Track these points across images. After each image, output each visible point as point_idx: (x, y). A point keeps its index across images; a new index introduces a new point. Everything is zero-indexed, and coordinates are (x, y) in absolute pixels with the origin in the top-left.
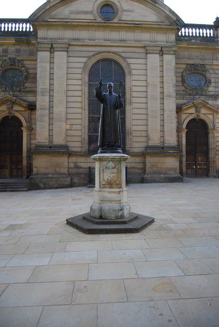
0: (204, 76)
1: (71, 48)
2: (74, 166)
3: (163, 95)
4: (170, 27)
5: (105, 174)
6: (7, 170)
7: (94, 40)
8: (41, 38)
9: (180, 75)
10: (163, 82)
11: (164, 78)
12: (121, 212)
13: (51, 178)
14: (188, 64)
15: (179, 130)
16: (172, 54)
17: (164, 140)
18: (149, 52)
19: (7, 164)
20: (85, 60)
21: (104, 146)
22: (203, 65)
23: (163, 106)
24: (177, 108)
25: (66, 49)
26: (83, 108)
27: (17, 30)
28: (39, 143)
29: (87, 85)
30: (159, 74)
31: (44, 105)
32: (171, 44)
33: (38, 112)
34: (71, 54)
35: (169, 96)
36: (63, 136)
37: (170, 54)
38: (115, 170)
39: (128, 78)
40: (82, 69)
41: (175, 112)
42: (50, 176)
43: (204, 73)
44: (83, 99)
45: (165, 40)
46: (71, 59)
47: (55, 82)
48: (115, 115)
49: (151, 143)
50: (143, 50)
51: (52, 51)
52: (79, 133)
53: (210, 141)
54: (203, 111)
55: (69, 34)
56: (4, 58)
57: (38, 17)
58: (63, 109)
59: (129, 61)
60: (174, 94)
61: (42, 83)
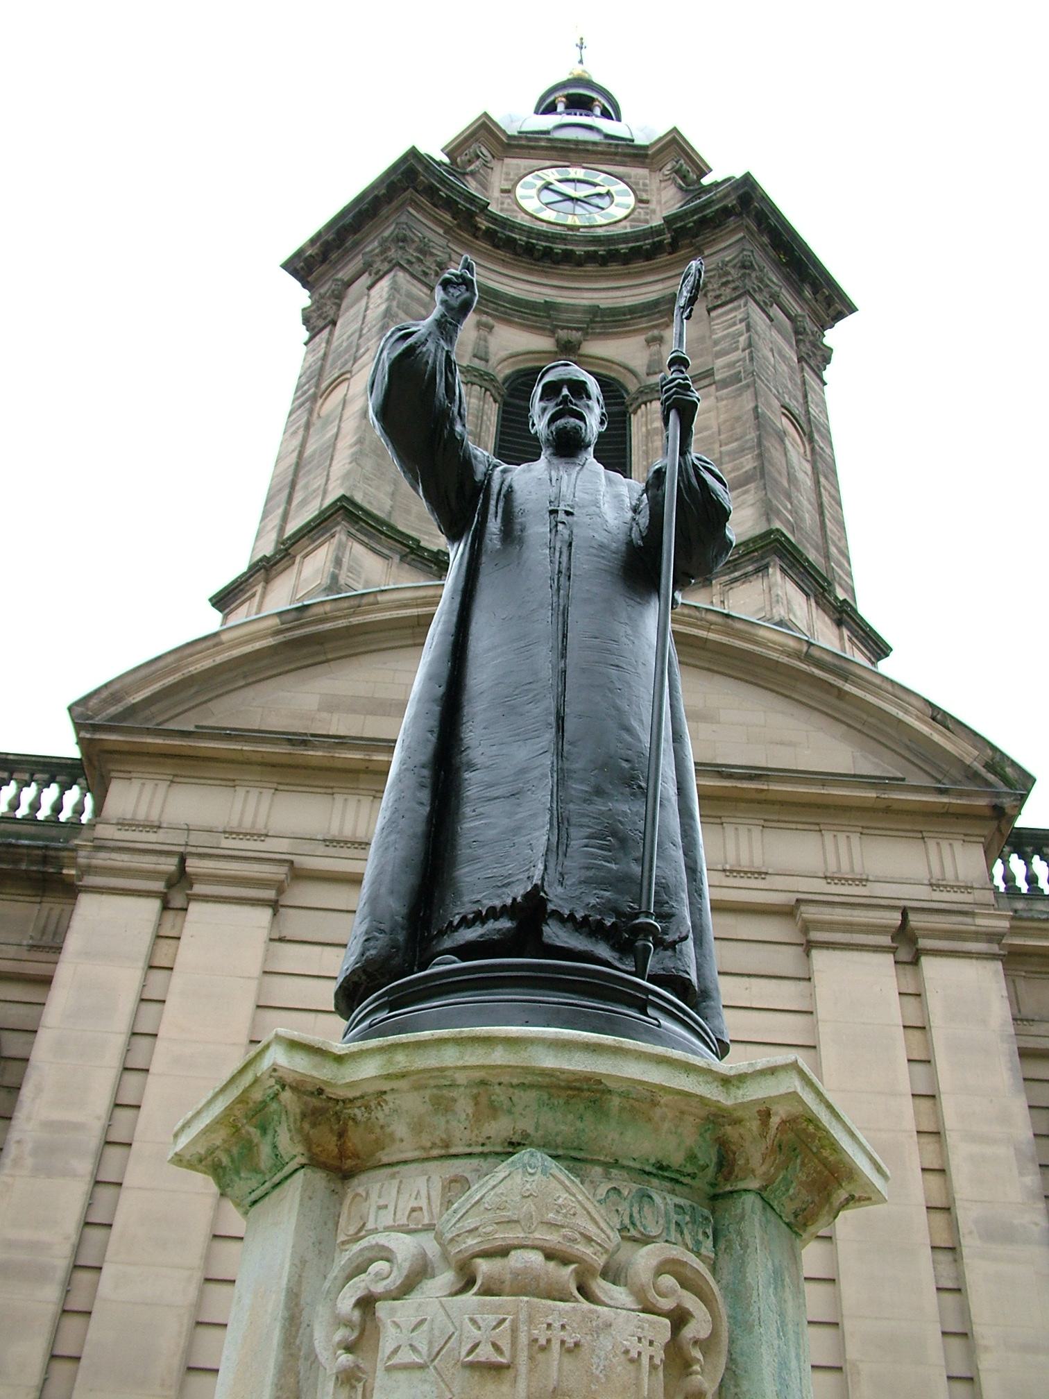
3: (954, 1227)
8: (122, 824)
10: (937, 1133)
18: (816, 936)
23: (964, 1312)
25: (270, 894)
30: (904, 1078)
31: (34, 1246)
34: (296, 923)
35: (1000, 1233)
37: (967, 955)
45: (923, 875)
51: (177, 901)
57: (132, 710)
58: (177, 1289)
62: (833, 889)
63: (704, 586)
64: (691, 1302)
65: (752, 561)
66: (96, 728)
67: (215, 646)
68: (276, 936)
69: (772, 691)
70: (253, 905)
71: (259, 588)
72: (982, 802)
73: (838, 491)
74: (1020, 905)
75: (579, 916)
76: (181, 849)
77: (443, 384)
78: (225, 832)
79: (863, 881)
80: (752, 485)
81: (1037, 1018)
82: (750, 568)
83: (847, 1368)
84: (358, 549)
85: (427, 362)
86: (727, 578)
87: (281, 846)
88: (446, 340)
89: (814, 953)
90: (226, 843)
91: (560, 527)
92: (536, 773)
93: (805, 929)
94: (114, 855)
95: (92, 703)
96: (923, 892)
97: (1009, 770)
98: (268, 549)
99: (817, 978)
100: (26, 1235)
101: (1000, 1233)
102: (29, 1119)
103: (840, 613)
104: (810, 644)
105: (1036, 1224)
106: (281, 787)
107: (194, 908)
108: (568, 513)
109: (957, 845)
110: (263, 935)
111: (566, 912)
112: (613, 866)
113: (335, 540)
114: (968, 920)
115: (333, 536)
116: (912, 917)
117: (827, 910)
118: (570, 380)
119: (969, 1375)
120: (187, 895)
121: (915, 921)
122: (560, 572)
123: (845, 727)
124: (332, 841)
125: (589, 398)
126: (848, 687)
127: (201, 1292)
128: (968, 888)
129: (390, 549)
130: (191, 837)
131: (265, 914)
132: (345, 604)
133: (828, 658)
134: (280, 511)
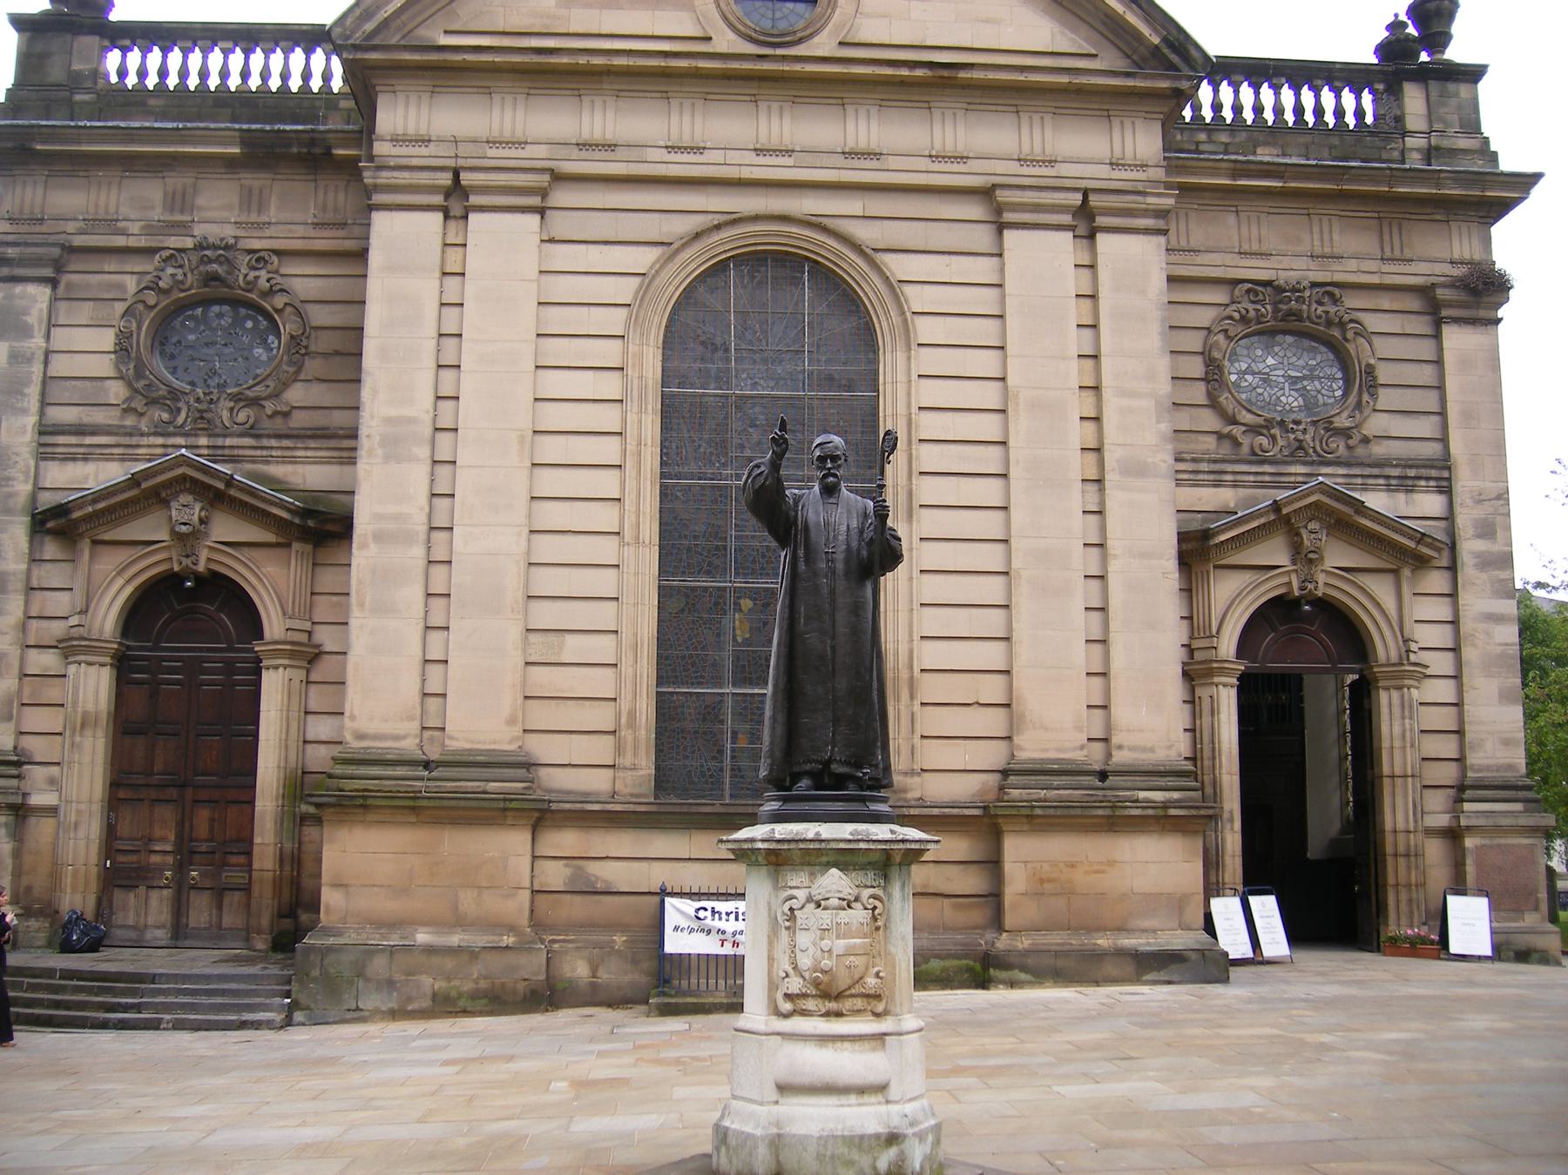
1: (563, 197)
2: (572, 879)
4: (1130, 83)
5: (803, 939)
6: (155, 895)
7: (699, 150)
8: (396, 140)
9: (1194, 342)
10: (1096, 388)
11: (1105, 362)
12: (893, 1152)
13: (430, 950)
14: (1236, 282)
15: (1195, 673)
16: (1147, 231)
17: (1108, 726)
18: (1009, 217)
19: (155, 859)
20: (644, 259)
21: (795, 778)
22: (1330, 291)
23: (1103, 529)
24: (1183, 537)
25: (535, 201)
26: (628, 534)
27: (254, 82)
28: (361, 736)
29: (654, 404)
31: (396, 517)
32: (1140, 175)
33: (364, 555)
34: (561, 224)
35: (1136, 470)
36: (508, 701)
38: (858, 915)
39: (893, 366)
40: (624, 311)
41: (1171, 564)
42: (422, 937)
43: (1336, 333)
44: (631, 484)
46: (563, 257)
47: (469, 385)
49: (1032, 747)
50: (974, 210)
51: (456, 210)
52: (601, 683)
54: (1338, 555)
55: (546, 125)
56: (174, 242)
57: (386, 23)
58: (511, 542)
59: (899, 267)
60: (1163, 459)
61: (393, 387)
62: (1026, 171)
64: (877, 903)
66: (356, 48)
74: (1202, 137)
76: (451, 163)
79: (1052, 162)
83: (1012, 573)
87: (541, 151)
89: (1006, 232)
90: (492, 152)
93: (999, 209)
94: (395, 174)
95: (349, 21)
96: (1104, 171)
99: (1006, 254)
100: (390, 509)
102: (372, 417)
107: (472, 217)
114: (1140, 199)
116: (1091, 197)
117: (1019, 193)
121: (1094, 200)
131: (535, 219)
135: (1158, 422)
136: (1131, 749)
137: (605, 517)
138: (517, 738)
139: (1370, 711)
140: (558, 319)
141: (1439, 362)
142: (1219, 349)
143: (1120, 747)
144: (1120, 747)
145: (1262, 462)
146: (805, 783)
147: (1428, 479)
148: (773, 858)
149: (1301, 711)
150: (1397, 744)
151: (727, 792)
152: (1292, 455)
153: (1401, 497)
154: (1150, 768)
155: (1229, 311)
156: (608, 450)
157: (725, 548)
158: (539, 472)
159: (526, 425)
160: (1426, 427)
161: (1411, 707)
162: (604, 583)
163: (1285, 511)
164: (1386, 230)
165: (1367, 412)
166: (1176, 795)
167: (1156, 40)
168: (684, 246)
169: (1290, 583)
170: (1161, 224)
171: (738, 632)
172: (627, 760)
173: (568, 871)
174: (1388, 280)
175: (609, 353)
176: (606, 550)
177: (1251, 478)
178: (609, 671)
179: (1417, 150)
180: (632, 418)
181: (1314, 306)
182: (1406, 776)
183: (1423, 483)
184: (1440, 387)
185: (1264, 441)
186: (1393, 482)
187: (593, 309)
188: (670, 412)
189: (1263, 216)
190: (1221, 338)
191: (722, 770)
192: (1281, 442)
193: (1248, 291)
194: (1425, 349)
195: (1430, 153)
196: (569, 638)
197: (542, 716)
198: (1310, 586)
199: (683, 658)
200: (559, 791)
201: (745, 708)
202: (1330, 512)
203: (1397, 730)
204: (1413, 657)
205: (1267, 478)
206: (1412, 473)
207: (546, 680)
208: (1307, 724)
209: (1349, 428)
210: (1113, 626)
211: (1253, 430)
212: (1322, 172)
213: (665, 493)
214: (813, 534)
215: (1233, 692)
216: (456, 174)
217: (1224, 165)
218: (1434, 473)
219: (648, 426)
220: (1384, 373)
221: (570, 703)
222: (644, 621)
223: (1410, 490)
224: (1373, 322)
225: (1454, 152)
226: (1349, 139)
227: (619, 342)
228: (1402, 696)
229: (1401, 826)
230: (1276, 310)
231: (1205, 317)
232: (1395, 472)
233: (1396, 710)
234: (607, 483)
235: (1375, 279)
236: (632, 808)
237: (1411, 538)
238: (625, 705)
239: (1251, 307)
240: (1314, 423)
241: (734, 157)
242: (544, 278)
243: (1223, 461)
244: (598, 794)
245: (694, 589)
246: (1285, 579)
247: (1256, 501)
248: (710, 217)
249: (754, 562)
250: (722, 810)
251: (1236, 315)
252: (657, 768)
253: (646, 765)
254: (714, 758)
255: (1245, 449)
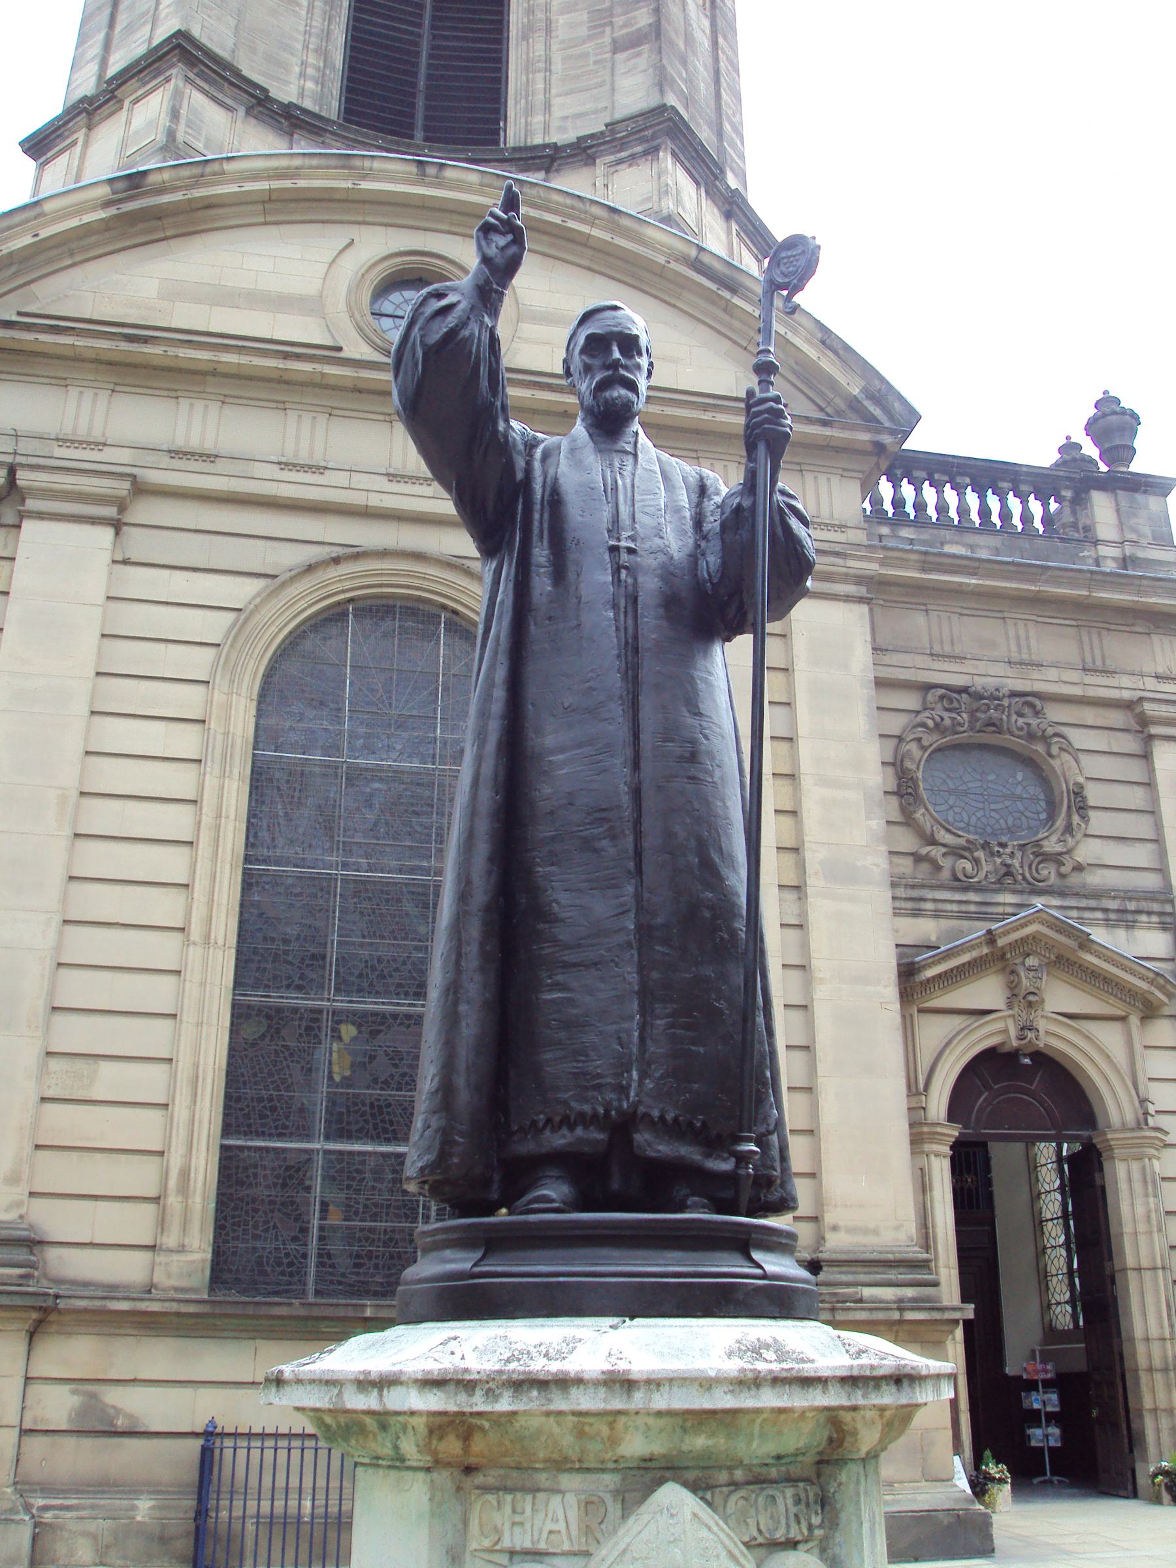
0: (1031, 763)
1: (146, 511)
3: (801, 867)
7: (320, 469)
11: (805, 748)
14: (928, 687)
15: (918, 1137)
16: (848, 599)
20: (242, 591)
22: (1031, 701)
23: (805, 946)
25: (111, 512)
26: (196, 933)
29: (241, 769)
34: (139, 543)
35: (843, 873)
37: (834, 597)
41: (889, 991)
43: (1040, 748)
44: (203, 868)
46: (139, 582)
48: (689, 698)
52: (144, 1129)
53: (1125, 1209)
54: (1061, 997)
55: (134, 425)
63: (586, 165)
65: (646, 140)
67: (35, 218)
68: (120, 559)
69: (656, 297)
70: (93, 523)
71: (80, 135)
72: (865, 437)
73: (737, 55)
74: (885, 530)
75: (670, 1116)
76: (9, 459)
77: (486, 374)
78: (57, 440)
80: (645, 48)
81: (890, 648)
82: (639, 149)
84: (198, 98)
85: (471, 352)
86: (612, 158)
88: (490, 316)
91: (624, 573)
92: (621, 938)
97: (897, 405)
98: (87, 86)
101: (843, 873)
103: (730, 203)
104: (701, 249)
105: (877, 866)
106: (118, 388)
107: (28, 526)
108: (631, 551)
109: (835, 480)
110: (106, 557)
111: (656, 1113)
112: (702, 1050)
113: (171, 86)
114: (839, 561)
115: (168, 80)
118: (620, 333)
119: (803, 1003)
120: (19, 511)
122: (627, 643)
123: (728, 343)
124: (177, 452)
125: (640, 354)
126: (736, 301)
127: (61, 934)
128: (842, 527)
129: (235, 99)
130: (19, 444)
131: (107, 533)
132: (185, 172)
133: (718, 266)
134: (101, 36)
135: (868, 818)
136: (851, 1231)
137: (164, 907)
138: (19, 1204)
139: (1103, 1188)
140: (126, 656)
141: (1150, 785)
142: (912, 759)
143: (835, 1228)
144: (835, 1228)
145: (966, 889)
146: (554, 1190)
147: (1149, 913)
148: (451, 1446)
149: (990, 1196)
150: (1142, 1228)
151: (311, 1286)
152: (999, 882)
153: (1121, 933)
154: (875, 1256)
155: (919, 719)
156: (176, 822)
157: (324, 957)
158: (82, 844)
159: (68, 775)
160: (1141, 855)
161: (1154, 1182)
162: (157, 993)
163: (1000, 943)
164: (1085, 638)
165: (1079, 836)
166: (909, 1292)
167: (856, 391)
168: (292, 579)
169: (1005, 1031)
170: (862, 591)
171: (336, 1069)
172: (171, 1240)
173: (75, 1401)
174: (1092, 692)
175: (189, 700)
176: (162, 950)
177: (955, 907)
178: (156, 1115)
179: (1113, 559)
180: (211, 782)
181: (1014, 717)
182: (1155, 1269)
183: (1144, 918)
184: (1153, 812)
185: (968, 866)
186: (1112, 916)
187: (171, 646)
188: (261, 780)
189: (955, 617)
190: (913, 747)
191: (305, 1256)
192: (986, 867)
193: (942, 697)
194: (1133, 770)
195: (1125, 562)
196: (105, 1067)
197: (59, 1173)
198: (1030, 1035)
199: (261, 1100)
200: (74, 1282)
201: (341, 1171)
202: (1050, 946)
203: (1140, 1210)
204: (1150, 1120)
205: (972, 908)
206: (1132, 906)
207: (66, 1123)
208: (997, 1211)
209: (1060, 854)
210: (821, 1068)
211: (955, 852)
212: (1019, 571)
213: (249, 882)
214: (574, 510)
215: (946, 1164)
216: (12, 470)
217: (914, 557)
218: (1156, 907)
219: (235, 796)
220: (1094, 795)
221: (98, 1156)
222: (208, 1046)
223: (1130, 926)
224: (1079, 739)
225: (1149, 563)
226: (1041, 543)
227: (201, 689)
228: (1143, 1169)
229: (1154, 1332)
230: (973, 719)
231: (896, 724)
232: (1113, 905)
233: (1138, 1187)
234: (172, 863)
235: (1077, 691)
236: (174, 1307)
237: (1142, 978)
238: (176, 1161)
239: (946, 715)
240: (1022, 847)
241: (360, 481)
242: (113, 605)
243: (923, 886)
244: (127, 1287)
245: (279, 1010)
246: (1000, 1025)
247: (961, 933)
248: (328, 549)
249: (360, 976)
250: (302, 1312)
251: (930, 723)
252: (217, 1252)
253: (198, 1248)
254: (295, 1239)
255: (945, 875)
